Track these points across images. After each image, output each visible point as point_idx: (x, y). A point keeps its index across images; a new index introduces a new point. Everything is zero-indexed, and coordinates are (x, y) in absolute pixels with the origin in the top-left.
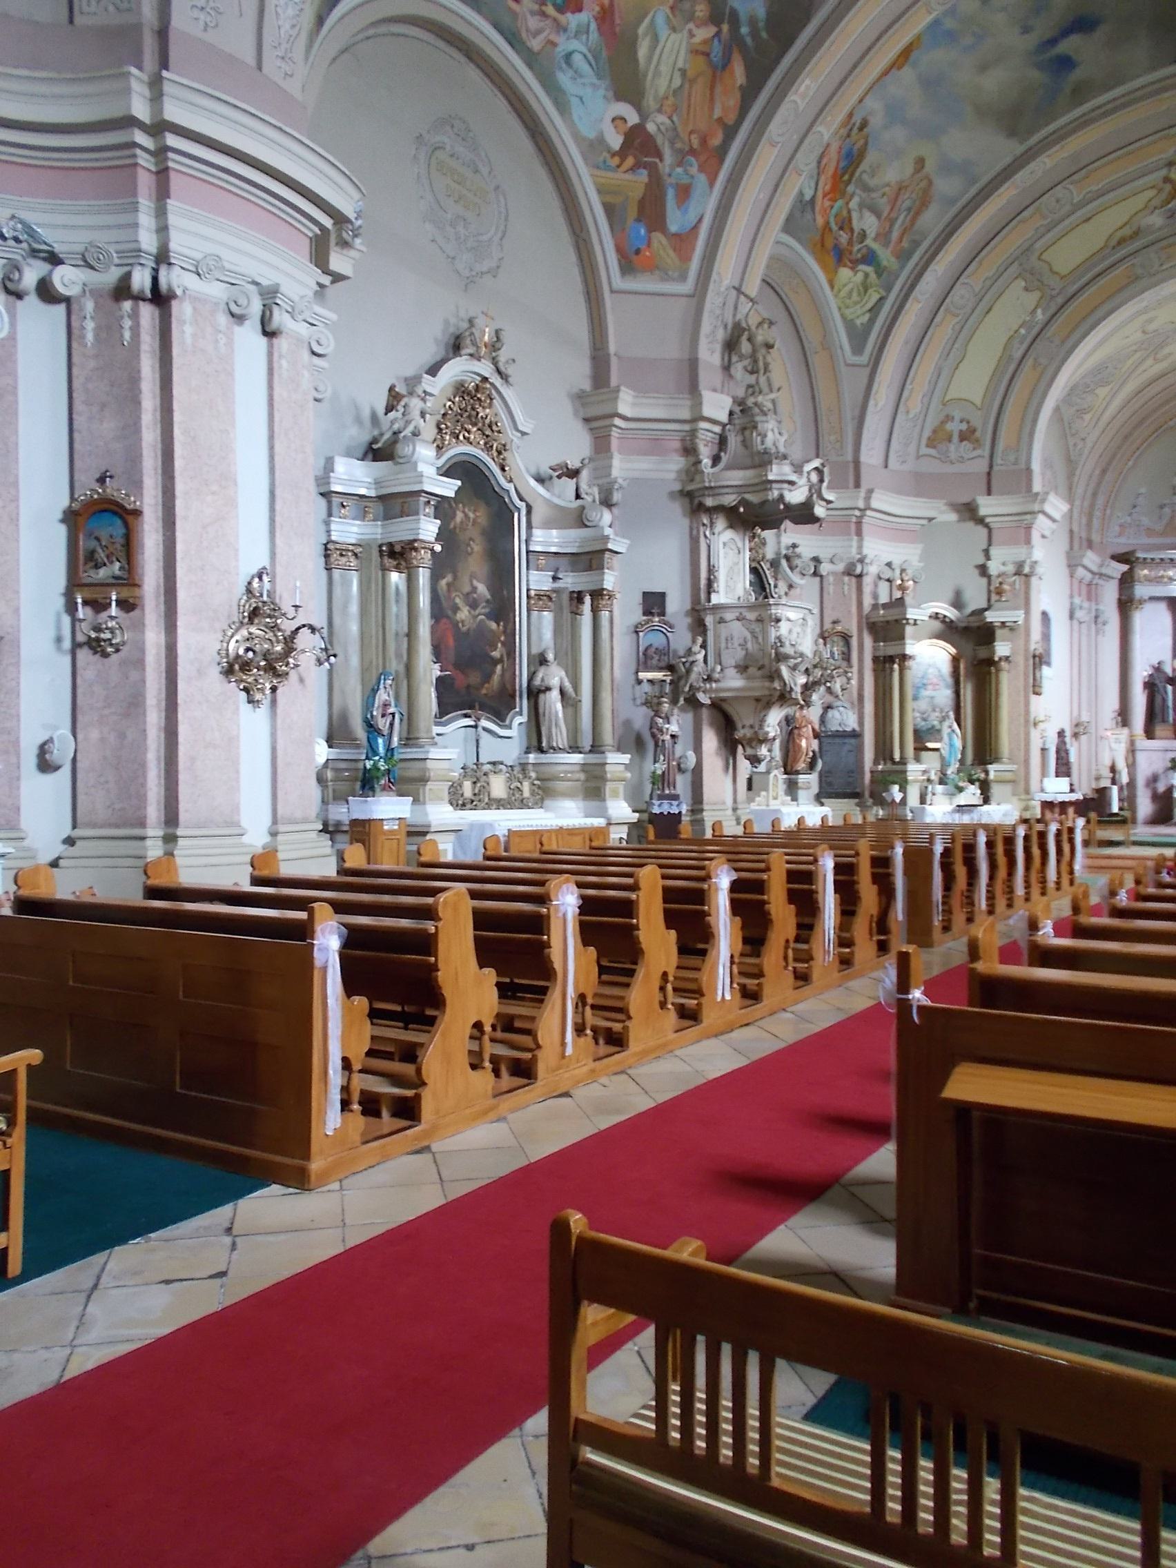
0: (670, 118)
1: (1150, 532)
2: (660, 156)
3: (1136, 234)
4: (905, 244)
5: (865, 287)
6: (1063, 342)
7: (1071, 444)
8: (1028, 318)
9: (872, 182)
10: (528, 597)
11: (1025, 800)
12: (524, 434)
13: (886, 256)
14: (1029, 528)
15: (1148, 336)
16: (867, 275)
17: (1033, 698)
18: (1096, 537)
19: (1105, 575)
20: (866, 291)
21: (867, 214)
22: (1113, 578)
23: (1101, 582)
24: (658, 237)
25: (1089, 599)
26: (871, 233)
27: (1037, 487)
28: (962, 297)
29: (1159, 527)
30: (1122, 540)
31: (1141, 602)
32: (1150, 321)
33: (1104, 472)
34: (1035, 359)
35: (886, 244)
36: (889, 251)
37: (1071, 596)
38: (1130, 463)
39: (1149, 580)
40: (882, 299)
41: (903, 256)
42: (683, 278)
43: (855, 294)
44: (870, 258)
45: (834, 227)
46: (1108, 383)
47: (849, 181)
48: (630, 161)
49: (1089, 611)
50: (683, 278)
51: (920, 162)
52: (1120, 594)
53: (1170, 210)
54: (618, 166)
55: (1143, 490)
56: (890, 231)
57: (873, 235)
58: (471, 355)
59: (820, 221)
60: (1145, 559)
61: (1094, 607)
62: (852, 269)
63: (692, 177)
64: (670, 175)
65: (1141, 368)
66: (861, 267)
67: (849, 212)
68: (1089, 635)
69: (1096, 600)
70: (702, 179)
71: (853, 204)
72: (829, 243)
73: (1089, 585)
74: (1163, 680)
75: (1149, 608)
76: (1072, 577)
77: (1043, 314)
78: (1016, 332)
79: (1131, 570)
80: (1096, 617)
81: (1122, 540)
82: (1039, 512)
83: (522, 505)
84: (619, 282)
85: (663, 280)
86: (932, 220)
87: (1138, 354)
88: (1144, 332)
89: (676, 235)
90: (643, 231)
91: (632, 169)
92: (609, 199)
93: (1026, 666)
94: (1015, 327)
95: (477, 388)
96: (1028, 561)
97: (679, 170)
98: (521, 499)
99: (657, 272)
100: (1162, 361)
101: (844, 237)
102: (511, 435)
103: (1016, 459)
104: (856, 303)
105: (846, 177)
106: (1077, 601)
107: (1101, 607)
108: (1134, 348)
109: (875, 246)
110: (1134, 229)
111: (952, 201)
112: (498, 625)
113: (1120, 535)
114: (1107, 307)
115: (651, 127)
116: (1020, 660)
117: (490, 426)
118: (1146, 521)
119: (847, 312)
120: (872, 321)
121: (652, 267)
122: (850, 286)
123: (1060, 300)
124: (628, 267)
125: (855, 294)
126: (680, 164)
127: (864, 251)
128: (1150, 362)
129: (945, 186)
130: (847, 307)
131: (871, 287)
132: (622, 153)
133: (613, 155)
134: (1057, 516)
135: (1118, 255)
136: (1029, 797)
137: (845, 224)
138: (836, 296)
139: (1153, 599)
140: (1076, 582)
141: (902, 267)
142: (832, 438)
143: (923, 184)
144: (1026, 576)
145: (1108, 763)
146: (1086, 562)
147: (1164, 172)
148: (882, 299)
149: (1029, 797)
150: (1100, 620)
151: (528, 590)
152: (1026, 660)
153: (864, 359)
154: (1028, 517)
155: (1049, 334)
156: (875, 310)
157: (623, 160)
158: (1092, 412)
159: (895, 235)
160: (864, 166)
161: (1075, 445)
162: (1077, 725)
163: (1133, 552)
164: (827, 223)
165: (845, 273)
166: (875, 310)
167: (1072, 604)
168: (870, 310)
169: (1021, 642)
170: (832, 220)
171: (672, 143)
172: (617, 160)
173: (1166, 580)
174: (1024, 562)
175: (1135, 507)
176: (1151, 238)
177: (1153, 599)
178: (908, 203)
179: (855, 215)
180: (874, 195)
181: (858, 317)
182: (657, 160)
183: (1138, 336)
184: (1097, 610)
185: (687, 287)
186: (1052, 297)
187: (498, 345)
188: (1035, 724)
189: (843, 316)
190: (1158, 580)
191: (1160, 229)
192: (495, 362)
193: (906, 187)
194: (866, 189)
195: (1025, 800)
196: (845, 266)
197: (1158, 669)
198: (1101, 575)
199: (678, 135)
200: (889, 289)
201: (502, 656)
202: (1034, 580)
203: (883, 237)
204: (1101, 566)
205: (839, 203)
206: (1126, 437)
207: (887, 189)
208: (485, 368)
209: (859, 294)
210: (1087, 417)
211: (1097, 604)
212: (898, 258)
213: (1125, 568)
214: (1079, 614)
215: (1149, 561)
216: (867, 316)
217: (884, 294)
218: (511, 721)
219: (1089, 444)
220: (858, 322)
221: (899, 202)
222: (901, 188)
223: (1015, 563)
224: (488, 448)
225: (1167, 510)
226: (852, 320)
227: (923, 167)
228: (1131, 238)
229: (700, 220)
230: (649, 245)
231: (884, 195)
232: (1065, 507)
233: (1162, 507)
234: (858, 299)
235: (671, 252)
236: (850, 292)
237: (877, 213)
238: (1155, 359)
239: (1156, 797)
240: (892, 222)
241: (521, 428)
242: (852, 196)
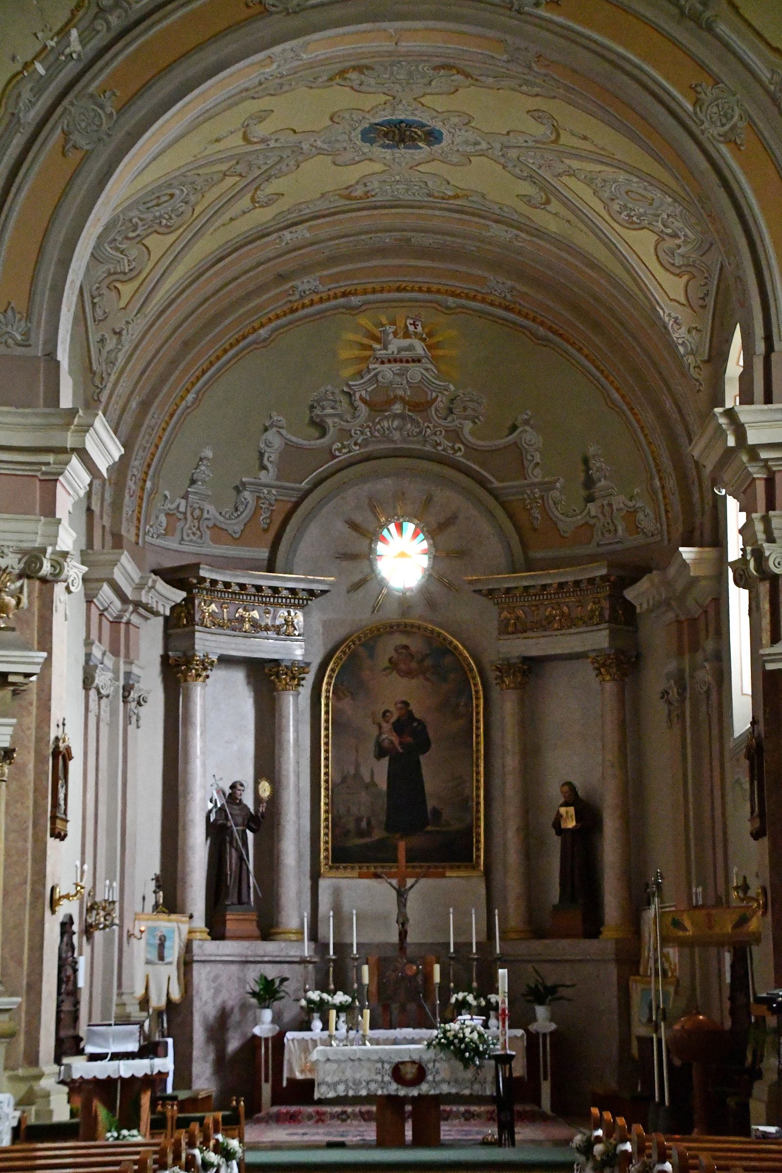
1: (219, 533)
6: (122, 110)
7: (93, 338)
8: (52, 43)
11: (22, 1079)
14: (50, 483)
15: (250, 148)
17: (51, 842)
18: (128, 532)
19: (146, 607)
22: (156, 614)
23: (135, 619)
25: (115, 652)
27: (66, 401)
29: (236, 527)
30: (172, 543)
31: (207, 664)
32: (262, 116)
33: (145, 405)
34: (66, 134)
37: (88, 643)
38: (190, 397)
39: (219, 624)
46: (169, 229)
49: (116, 672)
52: (166, 647)
55: (209, 453)
60: (214, 582)
61: (122, 668)
65: (226, 217)
68: (112, 725)
69: (127, 655)
73: (116, 623)
74: (240, 820)
75: (218, 675)
76: (89, 602)
77: (83, 42)
78: (26, 65)
79: (189, 601)
80: (127, 689)
81: (172, 543)
82: (73, 450)
87: (230, 181)
88: (246, 138)
93: (39, 774)
94: (21, 59)
96: (50, 550)
100: (267, 205)
103: (27, 334)
106: (97, 652)
107: (135, 670)
108: (224, 167)
113: (168, 532)
114: (210, 56)
116: (26, 758)
118: (211, 510)
128: (245, 202)
134: (103, 466)
136: (33, 1071)
139: (226, 661)
140: (95, 613)
144: (44, 580)
145: (140, 992)
146: (118, 575)
149: (33, 1071)
150: (133, 695)
152: (40, 759)
154: (51, 458)
155: (92, 89)
158: (136, 283)
161: (102, 341)
162: (90, 909)
163: (196, 566)
167: (88, 656)
169: (31, 721)
173: (247, 626)
174: (44, 551)
175: (193, 482)
177: (226, 661)
183: (237, 140)
184: (128, 674)
188: (53, 904)
190: (235, 626)
195: (22, 1079)
197: (233, 796)
198: (138, 604)
202: (59, 589)
204: (139, 587)
206: (187, 345)
210: (127, 290)
211: (129, 663)
213: (179, 595)
214: (102, 679)
215: (220, 586)
219: (127, 347)
223: (23, 552)
225: (246, 494)
232: (117, 451)
233: (238, 490)
238: (253, 200)
239: (221, 1064)
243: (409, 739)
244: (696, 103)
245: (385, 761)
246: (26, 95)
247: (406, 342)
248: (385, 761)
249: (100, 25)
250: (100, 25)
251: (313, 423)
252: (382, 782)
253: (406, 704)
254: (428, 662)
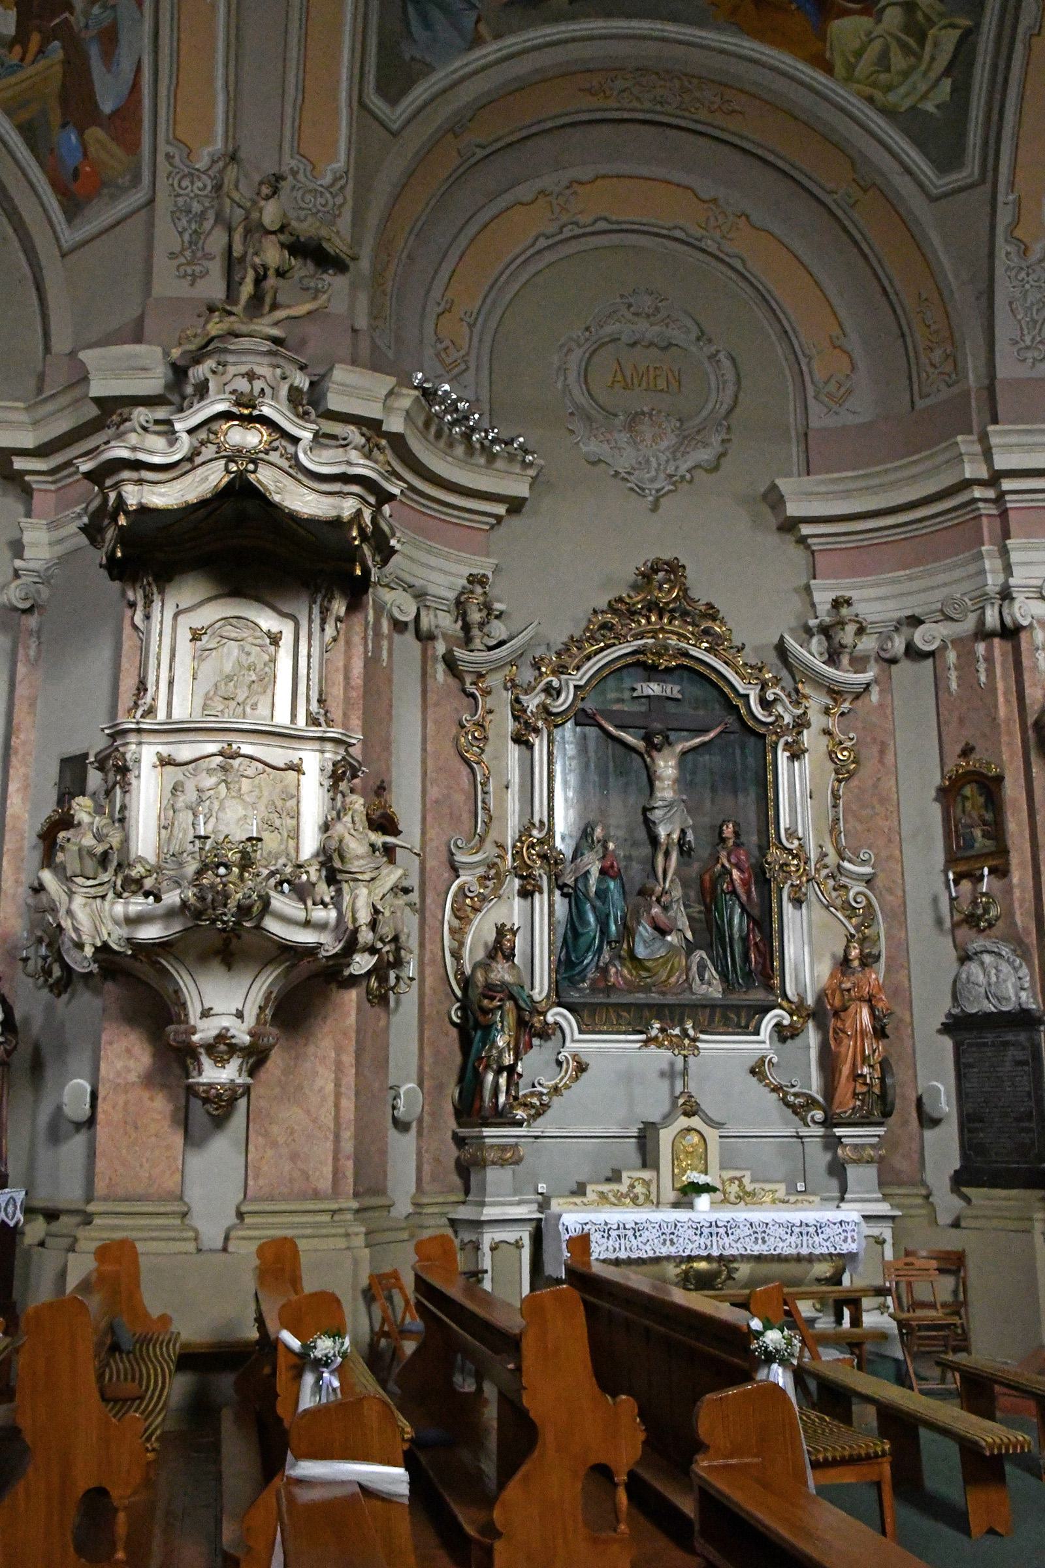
20: (922, 41)
40: (967, 38)
48: (35, 39)
54: (22, 60)
92: (24, 115)
104: (906, 74)
119: (892, 98)
120: (961, 91)
122: (877, 46)
125: (898, 61)
130: (889, 88)
131: (931, 23)
133: (11, 44)
138: (849, 79)
142: (937, 355)
148: (967, 38)
153: (971, 169)
168: (947, 72)
181: (924, 97)
189: (888, 112)
196: (846, 12)
216: (947, 84)
217: (966, 22)
220: (929, 107)
226: (913, 108)
234: (913, 60)
235: (114, 147)
236: (883, 62)
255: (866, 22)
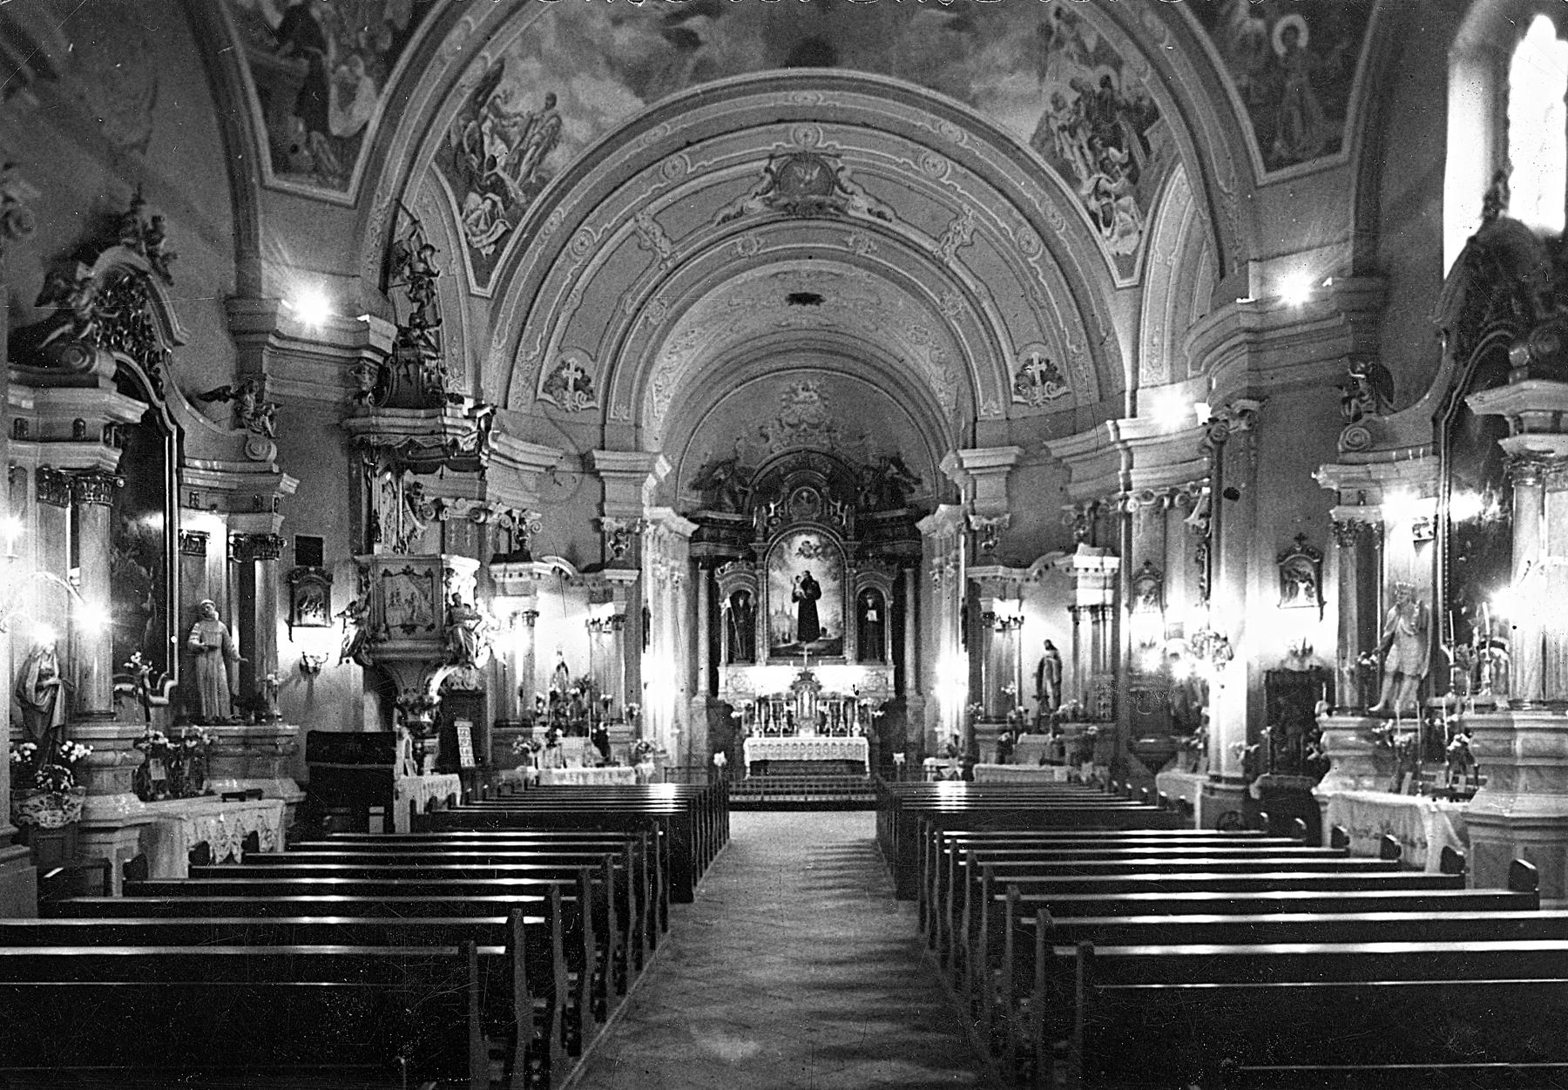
0: (337, 8)
2: (323, 46)
3: (741, 213)
4: (533, 179)
5: (492, 217)
9: (505, 109)
10: (180, 538)
12: (177, 344)
13: (513, 186)
16: (494, 204)
21: (498, 141)
24: (316, 136)
26: (501, 161)
28: (582, 244)
35: (514, 176)
36: (516, 185)
40: (508, 232)
41: (531, 191)
42: (344, 187)
43: (482, 222)
44: (498, 186)
45: (467, 150)
47: (482, 105)
48: (289, 46)
50: (344, 187)
51: (552, 99)
53: (768, 198)
56: (520, 162)
57: (503, 164)
58: (128, 245)
59: (454, 142)
62: (481, 195)
63: (358, 78)
64: (334, 72)
66: (490, 195)
67: (481, 135)
70: (367, 85)
71: (487, 126)
72: (462, 166)
83: (174, 429)
84: (271, 179)
85: (320, 184)
86: (560, 159)
89: (338, 138)
90: (301, 128)
91: (294, 55)
95: (131, 284)
97: (344, 68)
98: (173, 421)
99: (315, 176)
101: (475, 162)
102: (161, 343)
104: (483, 232)
105: (480, 99)
109: (501, 174)
110: (738, 208)
111: (579, 146)
112: (148, 570)
115: (315, 13)
117: (143, 333)
120: (497, 253)
121: (317, 170)
122: (479, 212)
123: (669, 264)
124: (283, 165)
126: (345, 62)
127: (493, 178)
129: (576, 129)
130: (474, 235)
132: (282, 33)
135: (721, 232)
137: (477, 148)
141: (529, 203)
143: (553, 121)
147: (765, 163)
148: (508, 232)
151: (180, 531)
156: (500, 242)
157: (282, 42)
159: (524, 168)
160: (498, 90)
164: (460, 144)
165: (474, 198)
166: (500, 242)
168: (496, 242)
170: (465, 140)
171: (337, 37)
172: (274, 42)
176: (750, 221)
178: (537, 137)
179: (487, 140)
180: (504, 123)
182: (319, 51)
185: (349, 197)
186: (664, 260)
187: (156, 236)
189: (468, 243)
191: (759, 215)
192: (152, 255)
193: (537, 120)
194: (499, 115)
199: (343, 29)
200: (515, 222)
201: (152, 608)
203: (514, 169)
205: (472, 124)
207: (518, 119)
208: (144, 263)
209: (486, 223)
212: (524, 192)
216: (493, 247)
218: (162, 686)
220: (484, 253)
221: (530, 134)
222: (532, 120)
224: (139, 359)
227: (554, 104)
228: (735, 217)
229: (365, 126)
230: (308, 142)
231: (515, 124)
237: (506, 140)
240: (522, 154)
241: (177, 337)
242: (486, 118)
243: (809, 591)
244: (942, 300)
245: (797, 604)
246: (629, 301)
247: (807, 394)
248: (797, 604)
249: (663, 266)
250: (663, 266)
251: (762, 435)
252: (796, 615)
253: (808, 572)
254: (819, 550)
255: (479, 200)
